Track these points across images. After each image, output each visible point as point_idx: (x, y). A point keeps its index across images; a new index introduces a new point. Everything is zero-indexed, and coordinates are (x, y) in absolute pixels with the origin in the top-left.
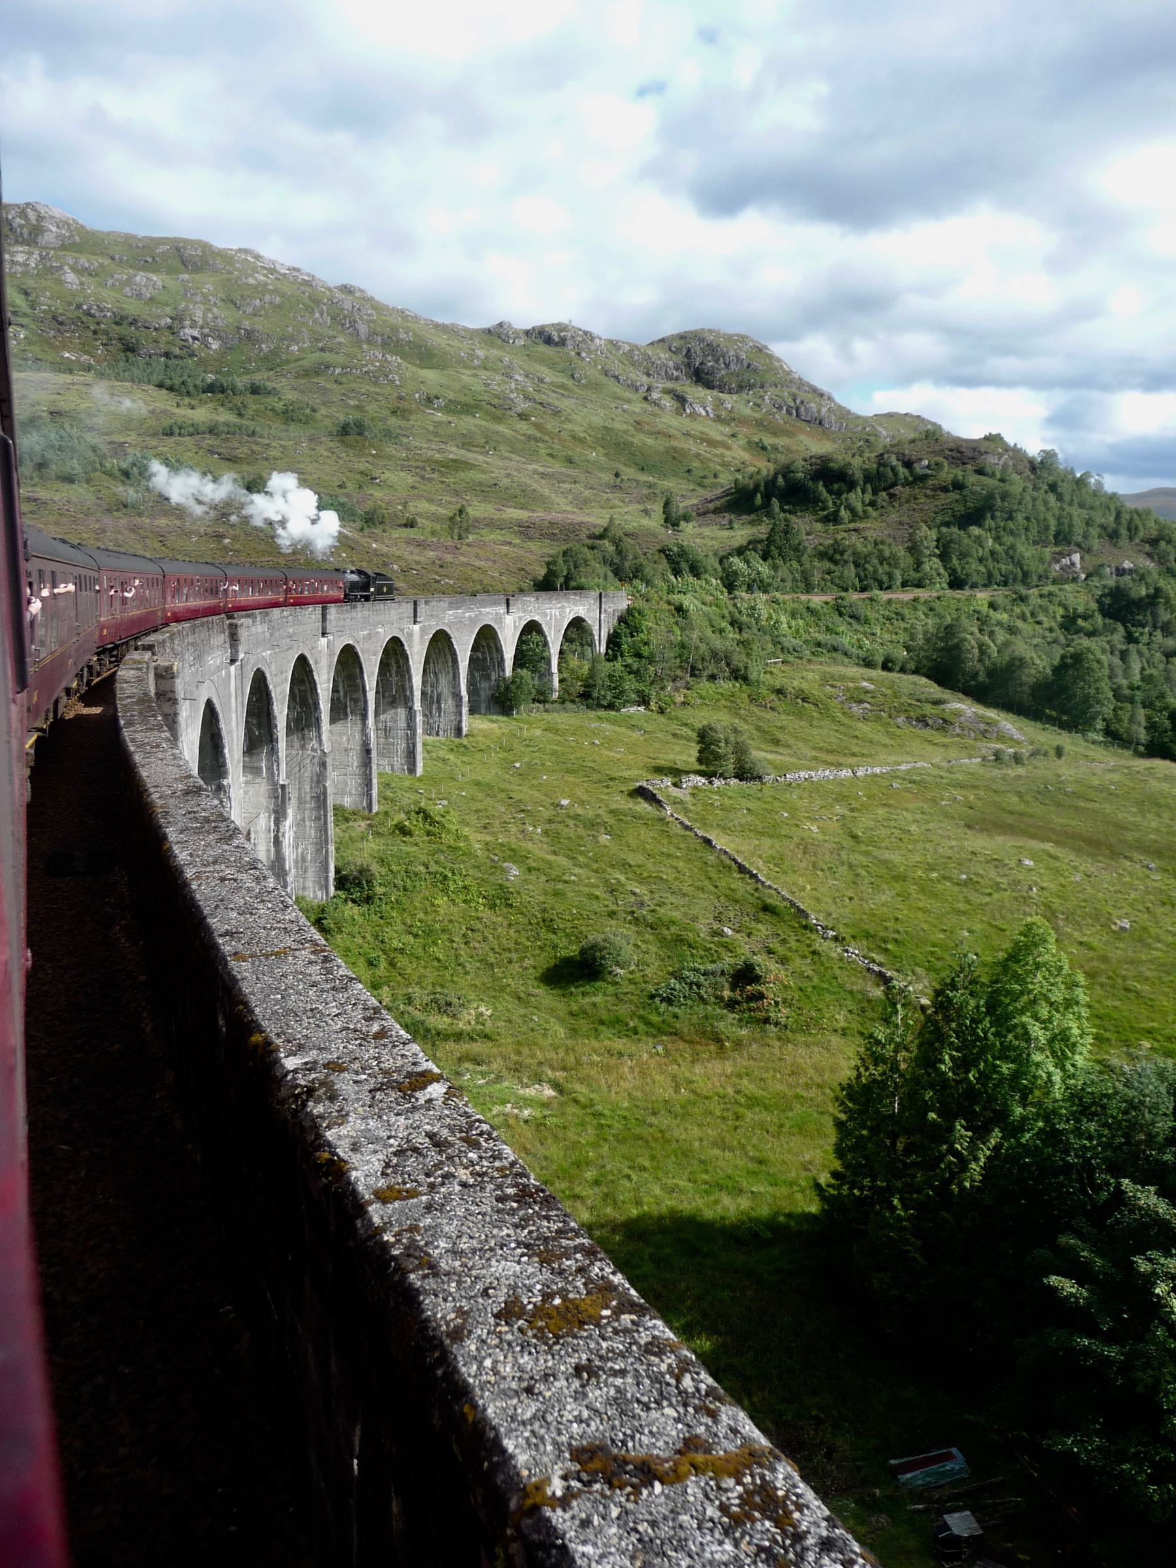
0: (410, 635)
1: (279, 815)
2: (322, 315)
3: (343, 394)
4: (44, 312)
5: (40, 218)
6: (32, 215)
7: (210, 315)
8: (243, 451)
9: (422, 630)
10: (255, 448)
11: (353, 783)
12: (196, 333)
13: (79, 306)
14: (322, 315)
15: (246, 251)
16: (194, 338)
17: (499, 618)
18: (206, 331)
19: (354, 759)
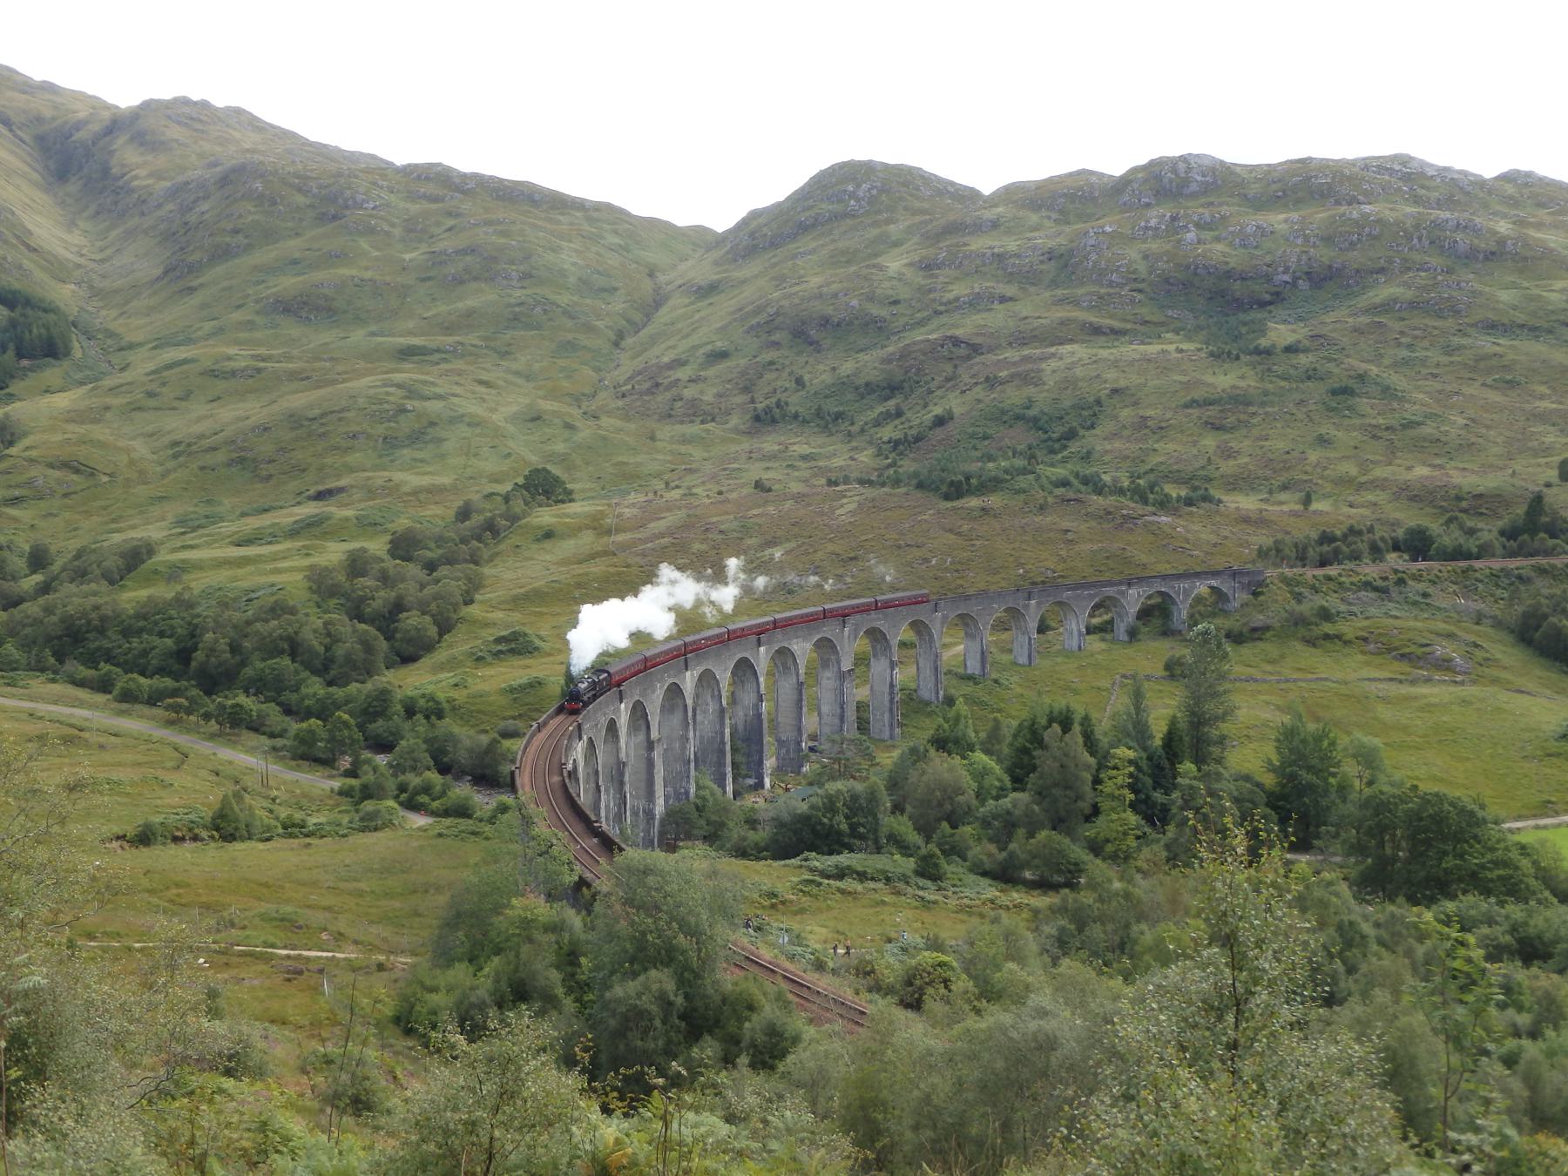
0: (1027, 606)
1: (892, 670)
2: (1420, 239)
3: (1402, 333)
4: (1159, 276)
5: (1189, 169)
6: (1182, 166)
7: (1304, 257)
8: (1231, 420)
9: (1039, 604)
10: (1242, 417)
11: (978, 666)
12: (1287, 278)
13: (1188, 267)
14: (1420, 239)
15: (1395, 158)
16: (1287, 282)
17: (1123, 593)
18: (1298, 274)
19: (979, 656)
